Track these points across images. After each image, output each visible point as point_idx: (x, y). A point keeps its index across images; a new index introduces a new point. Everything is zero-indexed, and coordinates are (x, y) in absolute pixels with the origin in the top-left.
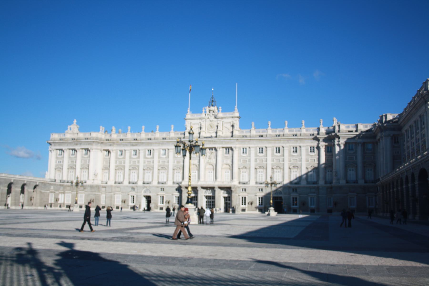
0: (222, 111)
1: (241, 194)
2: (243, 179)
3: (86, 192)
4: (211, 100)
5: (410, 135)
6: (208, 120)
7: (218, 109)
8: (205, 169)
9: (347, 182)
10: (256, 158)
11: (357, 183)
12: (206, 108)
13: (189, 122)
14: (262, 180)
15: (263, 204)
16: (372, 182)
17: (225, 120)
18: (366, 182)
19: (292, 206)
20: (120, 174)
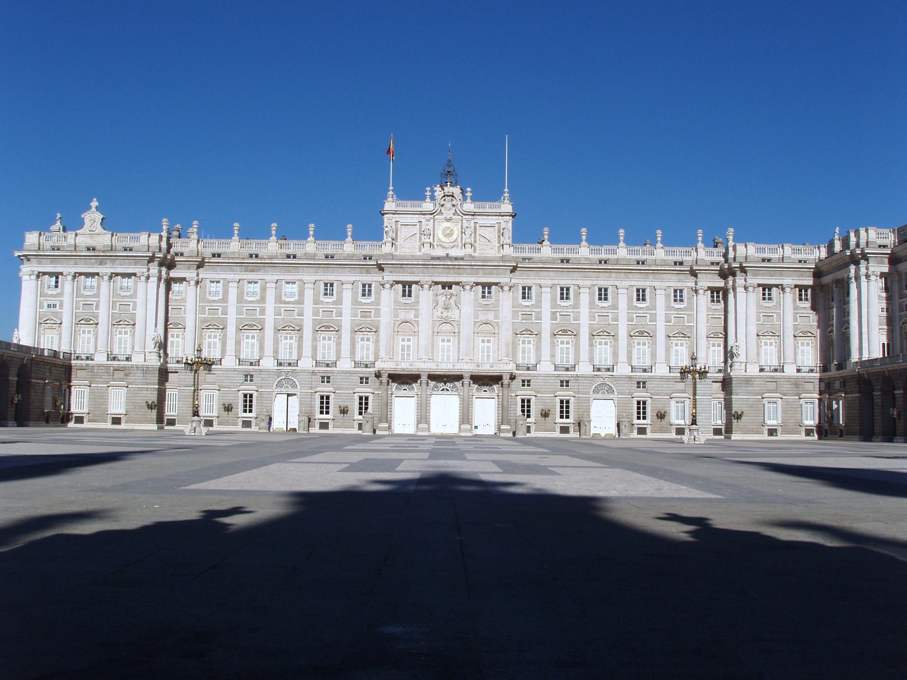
0: (474, 199)
1: (519, 393)
3: (129, 383)
6: (441, 217)
7: (463, 192)
10: (554, 310)
11: (783, 372)
12: (435, 189)
13: (394, 220)
14: (569, 362)
15: (571, 415)
16: (812, 371)
17: (481, 220)
18: (798, 371)
20: (212, 340)
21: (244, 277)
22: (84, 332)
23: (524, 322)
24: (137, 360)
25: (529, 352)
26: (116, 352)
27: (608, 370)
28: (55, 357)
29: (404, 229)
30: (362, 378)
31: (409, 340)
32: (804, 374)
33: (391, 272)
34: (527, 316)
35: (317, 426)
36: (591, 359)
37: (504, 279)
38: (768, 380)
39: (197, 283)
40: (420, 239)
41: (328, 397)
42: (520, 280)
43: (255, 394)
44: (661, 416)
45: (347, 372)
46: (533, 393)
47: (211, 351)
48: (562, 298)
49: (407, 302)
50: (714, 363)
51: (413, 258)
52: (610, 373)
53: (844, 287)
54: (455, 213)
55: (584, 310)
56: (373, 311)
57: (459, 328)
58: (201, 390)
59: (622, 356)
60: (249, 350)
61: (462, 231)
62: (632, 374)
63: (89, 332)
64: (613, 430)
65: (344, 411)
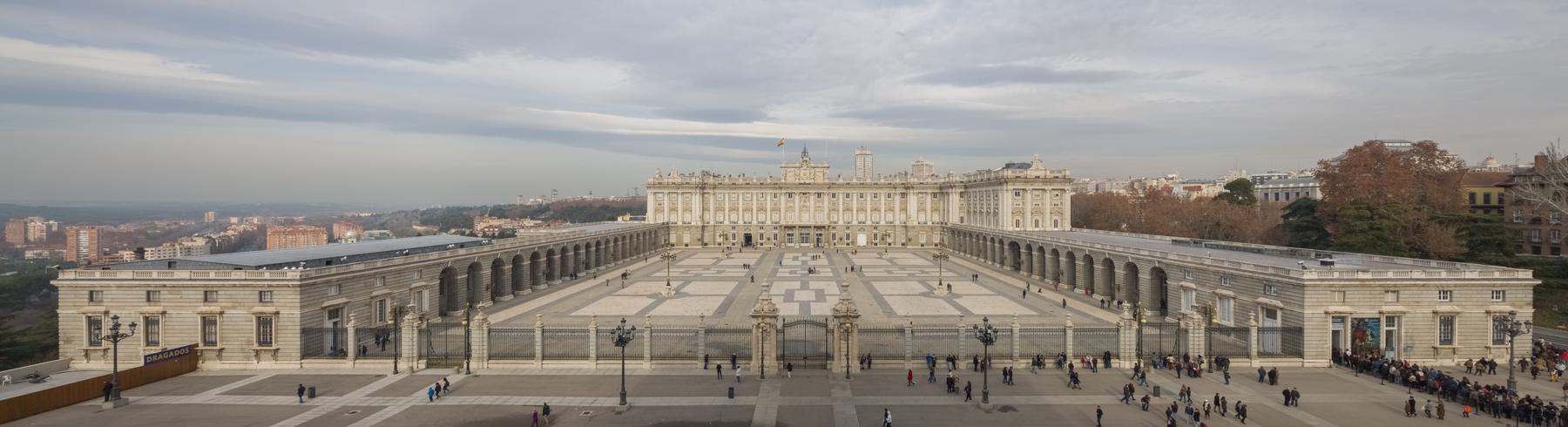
24: (693, 223)
34: (834, 204)
36: (857, 219)
42: (832, 191)
55: (855, 202)
59: (869, 218)
60: (734, 217)
64: (865, 244)
65: (769, 239)
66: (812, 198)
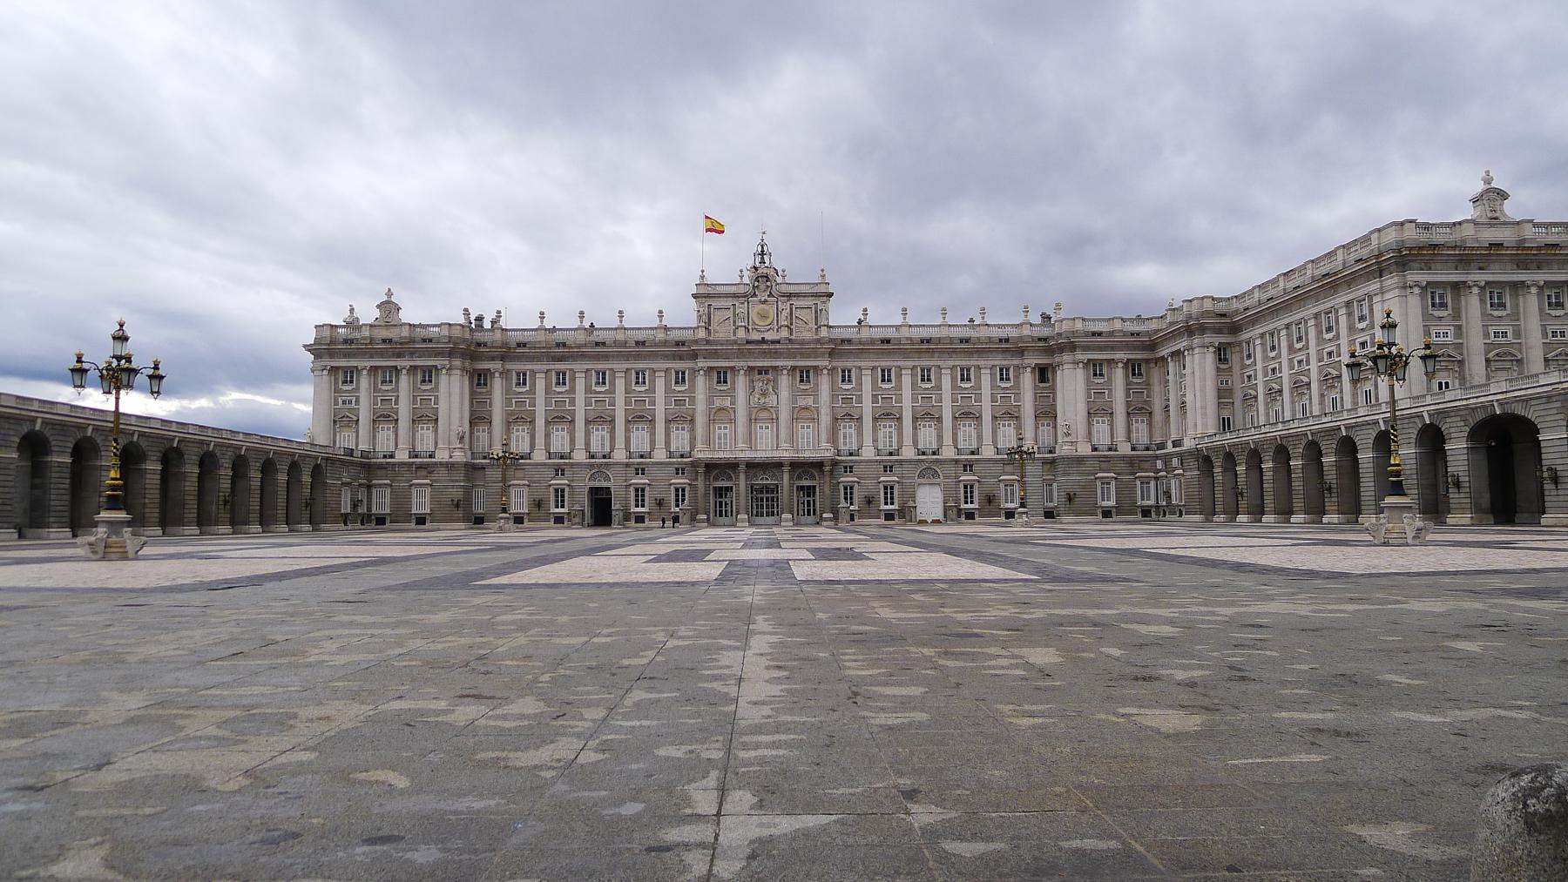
1: (842, 479)
2: (845, 444)
4: (760, 250)
5: (1284, 344)
8: (751, 420)
9: (1095, 449)
11: (1116, 450)
15: (896, 501)
17: (797, 302)
18: (1133, 449)
19: (963, 506)
20: (520, 433)
21: (553, 367)
22: (383, 429)
23: (844, 406)
24: (442, 456)
25: (851, 437)
26: (418, 448)
27: (934, 453)
28: (352, 456)
29: (718, 313)
30: (677, 469)
31: (725, 428)
32: (1139, 453)
33: (705, 358)
34: (847, 400)
35: (633, 520)
36: (915, 443)
37: (823, 362)
38: (1101, 459)
39: (501, 373)
40: (734, 322)
41: (643, 490)
42: (840, 364)
43: (567, 489)
44: (990, 499)
45: (662, 463)
46: (856, 479)
47: (517, 446)
48: (883, 380)
49: (722, 388)
50: (1044, 443)
51: (728, 342)
52: (935, 457)
53: (1179, 361)
54: (771, 295)
56: (687, 399)
57: (777, 415)
58: (509, 486)
60: (560, 441)
61: (777, 314)
62: (957, 457)
63: (389, 429)
65: (660, 503)
66: (784, 381)
